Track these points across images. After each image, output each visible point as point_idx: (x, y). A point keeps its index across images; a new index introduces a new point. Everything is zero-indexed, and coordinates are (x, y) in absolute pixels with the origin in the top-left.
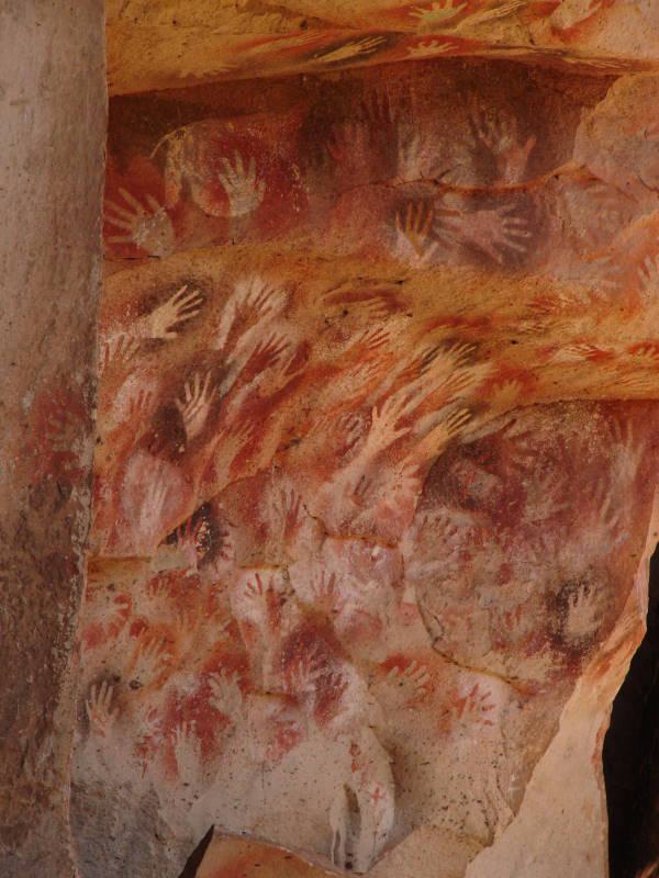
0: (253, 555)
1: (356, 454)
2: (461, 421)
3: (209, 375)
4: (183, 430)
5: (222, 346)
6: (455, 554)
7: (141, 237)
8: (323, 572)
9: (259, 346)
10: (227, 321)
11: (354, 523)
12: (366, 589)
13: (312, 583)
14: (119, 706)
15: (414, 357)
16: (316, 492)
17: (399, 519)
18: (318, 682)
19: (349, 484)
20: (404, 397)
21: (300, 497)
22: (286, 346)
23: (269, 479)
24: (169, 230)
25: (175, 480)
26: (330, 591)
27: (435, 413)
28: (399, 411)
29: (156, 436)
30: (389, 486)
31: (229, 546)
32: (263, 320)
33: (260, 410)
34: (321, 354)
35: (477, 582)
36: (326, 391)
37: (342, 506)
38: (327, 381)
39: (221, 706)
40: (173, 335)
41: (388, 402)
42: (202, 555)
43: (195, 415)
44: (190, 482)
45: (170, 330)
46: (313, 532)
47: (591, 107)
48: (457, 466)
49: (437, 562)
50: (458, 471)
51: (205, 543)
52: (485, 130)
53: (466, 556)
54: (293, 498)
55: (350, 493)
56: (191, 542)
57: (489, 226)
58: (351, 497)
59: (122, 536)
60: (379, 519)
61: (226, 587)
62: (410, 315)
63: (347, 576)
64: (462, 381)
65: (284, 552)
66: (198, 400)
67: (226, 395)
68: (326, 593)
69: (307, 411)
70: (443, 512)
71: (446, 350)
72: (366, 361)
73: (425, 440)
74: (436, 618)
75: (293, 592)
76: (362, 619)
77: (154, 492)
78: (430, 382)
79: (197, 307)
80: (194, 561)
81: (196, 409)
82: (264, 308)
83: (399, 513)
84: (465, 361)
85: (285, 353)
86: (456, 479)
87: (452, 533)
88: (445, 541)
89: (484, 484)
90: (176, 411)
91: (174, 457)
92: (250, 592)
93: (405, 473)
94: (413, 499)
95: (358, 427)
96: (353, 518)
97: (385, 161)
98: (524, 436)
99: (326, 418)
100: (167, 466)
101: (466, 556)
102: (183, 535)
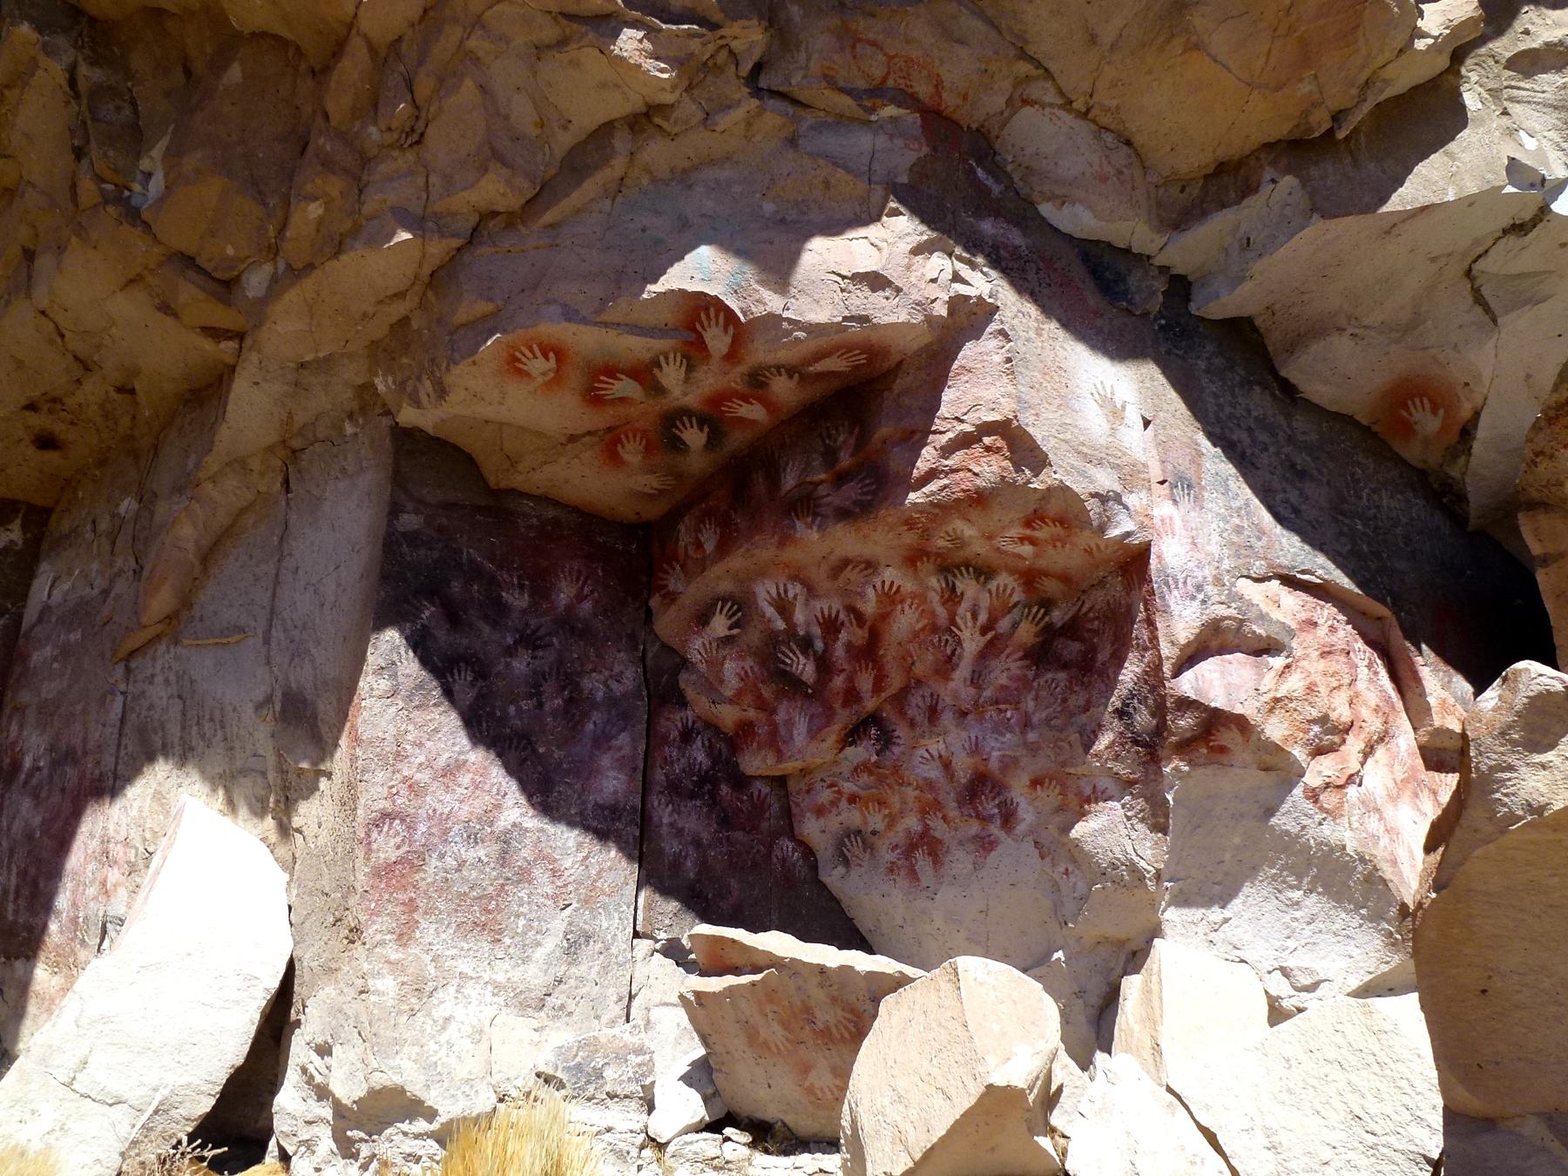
1: (960, 658)
7: (671, 588)
10: (770, 611)
14: (868, 847)
18: (998, 806)
20: (969, 615)
24: (682, 576)
30: (997, 672)
33: (868, 652)
34: (869, 606)
35: (1072, 715)
37: (967, 693)
39: (937, 835)
40: (735, 631)
41: (958, 619)
45: (730, 628)
47: (890, 389)
52: (829, 437)
53: (1065, 700)
57: (851, 491)
67: (825, 651)
70: (1049, 676)
72: (902, 601)
78: (976, 599)
79: (738, 610)
82: (791, 594)
85: (842, 616)
89: (1072, 649)
91: (807, 696)
97: (774, 481)
98: (1090, 609)
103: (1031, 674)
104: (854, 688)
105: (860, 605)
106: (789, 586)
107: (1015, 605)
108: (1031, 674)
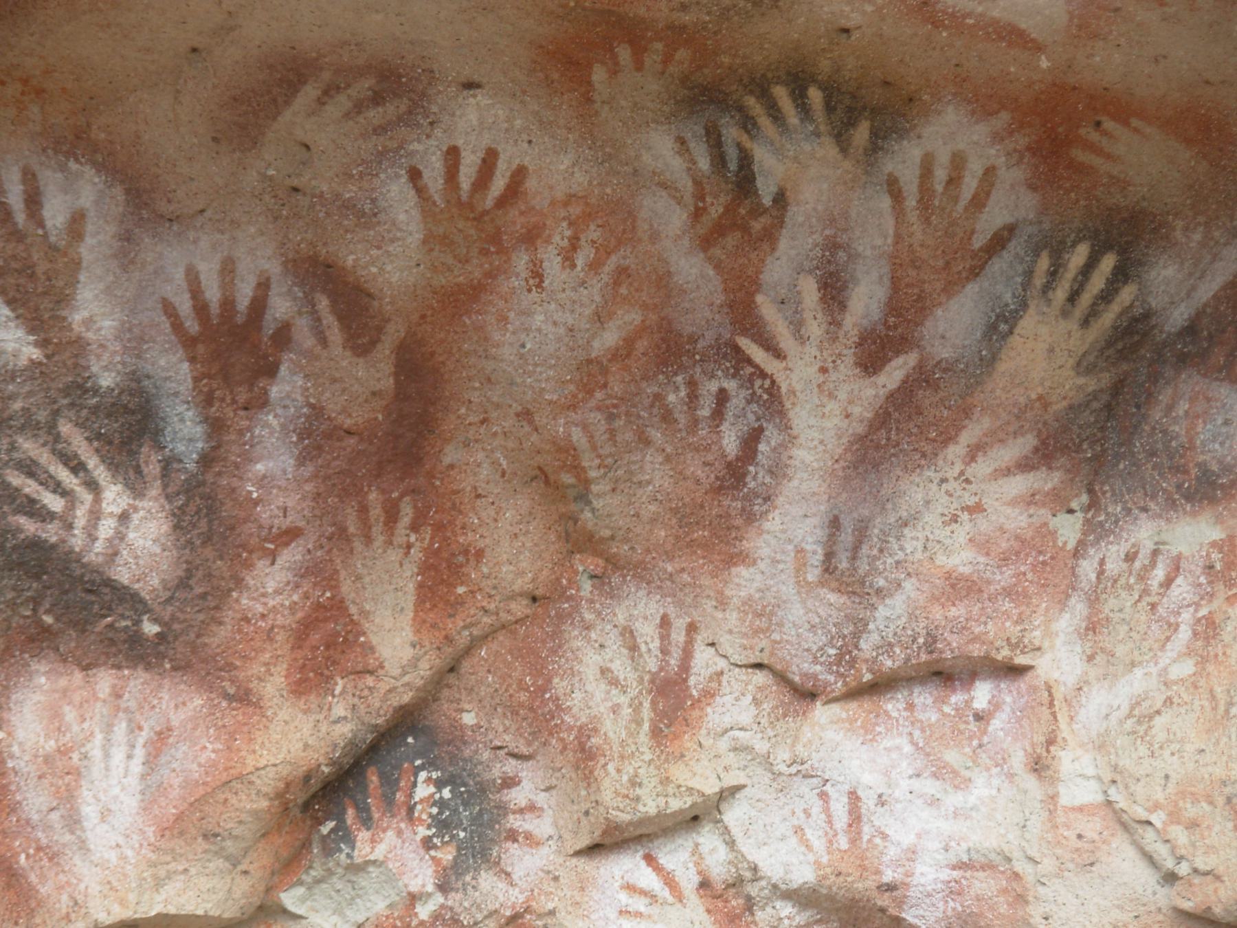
0: (587, 813)
1: (778, 471)
2: (1097, 282)
3: (65, 428)
4: (109, 583)
5: (36, 354)
6: (1185, 633)
8: (823, 796)
9: (169, 309)
11: (867, 645)
12: (972, 800)
13: (799, 830)
15: (686, 185)
16: (722, 603)
17: (1008, 592)
19: (800, 551)
20: (810, 290)
21: (692, 628)
22: (264, 286)
23: (576, 609)
25: (178, 704)
26: (853, 841)
27: (972, 288)
28: (835, 323)
29: (48, 619)
30: (931, 519)
31: (532, 808)
32: (95, 246)
36: (508, 353)
38: (480, 328)
42: (447, 855)
43: (120, 536)
44: (244, 698)
46: (756, 702)
48: (1164, 397)
49: (1138, 672)
50: (1170, 408)
51: (443, 825)
54: (665, 637)
55: (812, 575)
56: (400, 833)
58: (822, 584)
59: (43, 890)
60: (937, 613)
61: (552, 913)
62: (470, 85)
63: (905, 784)
64: (953, 181)
65: (666, 781)
66: (97, 500)
67: (206, 460)
68: (843, 843)
69: (526, 415)
70: (1144, 533)
71: (748, 124)
72: (531, 237)
73: (1002, 367)
74: (1149, 823)
75: (755, 869)
76: (983, 885)
77: (107, 756)
80: (421, 876)
81: (106, 528)
82: (55, 213)
83: (1004, 577)
84: (861, 134)
85: (280, 307)
86: (1165, 432)
87: (1168, 583)
88: (1153, 606)
90: (36, 544)
92: (640, 904)
93: (982, 467)
94: (1046, 533)
95: (737, 401)
96: (857, 635)
99: (596, 417)
100: (137, 682)
101: (1208, 629)
102: (366, 821)
103: (1068, 529)
104: (337, 607)
105: (354, 256)
106: (50, 180)
107: (999, 242)
108: (1068, 529)
